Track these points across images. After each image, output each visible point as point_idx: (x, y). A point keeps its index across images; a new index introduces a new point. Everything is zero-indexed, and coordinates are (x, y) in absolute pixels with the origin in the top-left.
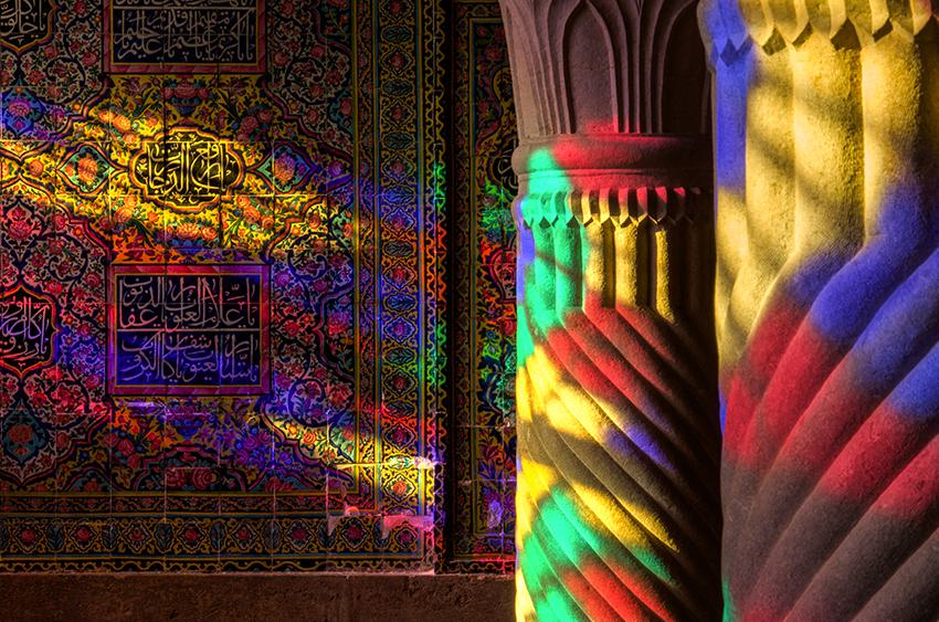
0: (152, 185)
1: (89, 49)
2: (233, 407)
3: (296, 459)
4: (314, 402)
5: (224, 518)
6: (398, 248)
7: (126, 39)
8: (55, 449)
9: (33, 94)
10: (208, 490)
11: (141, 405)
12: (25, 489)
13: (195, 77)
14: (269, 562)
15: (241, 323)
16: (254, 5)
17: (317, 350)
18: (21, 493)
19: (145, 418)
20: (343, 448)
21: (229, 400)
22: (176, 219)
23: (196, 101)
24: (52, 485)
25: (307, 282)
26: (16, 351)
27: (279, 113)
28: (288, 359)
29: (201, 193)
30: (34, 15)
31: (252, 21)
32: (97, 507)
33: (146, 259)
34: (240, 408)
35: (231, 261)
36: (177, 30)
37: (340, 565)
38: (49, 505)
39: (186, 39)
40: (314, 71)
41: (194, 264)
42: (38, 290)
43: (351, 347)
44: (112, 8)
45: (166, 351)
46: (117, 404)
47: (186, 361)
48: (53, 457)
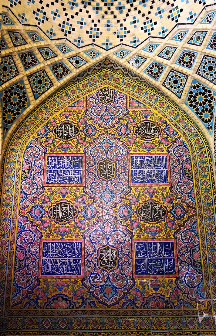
0: (143, 217)
1: (125, 180)
2: (169, 282)
3: (188, 298)
4: (192, 280)
5: (168, 318)
6: (211, 234)
7: (135, 178)
8: (118, 295)
9: (111, 192)
10: (163, 308)
11: (142, 281)
12: (110, 308)
13: (153, 187)
14: (183, 332)
15: (169, 256)
16: (167, 169)
17: (191, 264)
18: (109, 309)
19: (144, 285)
20: (201, 294)
21: (167, 279)
22: (150, 226)
23: (153, 194)
24: (118, 307)
25: (187, 244)
26: (107, 264)
27: (176, 197)
28: (183, 267)
29: (156, 218)
30: (111, 171)
31: (167, 172)
32: (131, 314)
33: (142, 237)
34: (171, 282)
35: (165, 238)
36: (148, 175)
37: (204, 333)
38: (117, 313)
39: (150, 177)
40: (184, 185)
41: (155, 239)
42: (113, 246)
43: (201, 263)
44: (131, 169)
45: (149, 264)
46: (136, 281)
47: (155, 267)
48: (118, 298)
